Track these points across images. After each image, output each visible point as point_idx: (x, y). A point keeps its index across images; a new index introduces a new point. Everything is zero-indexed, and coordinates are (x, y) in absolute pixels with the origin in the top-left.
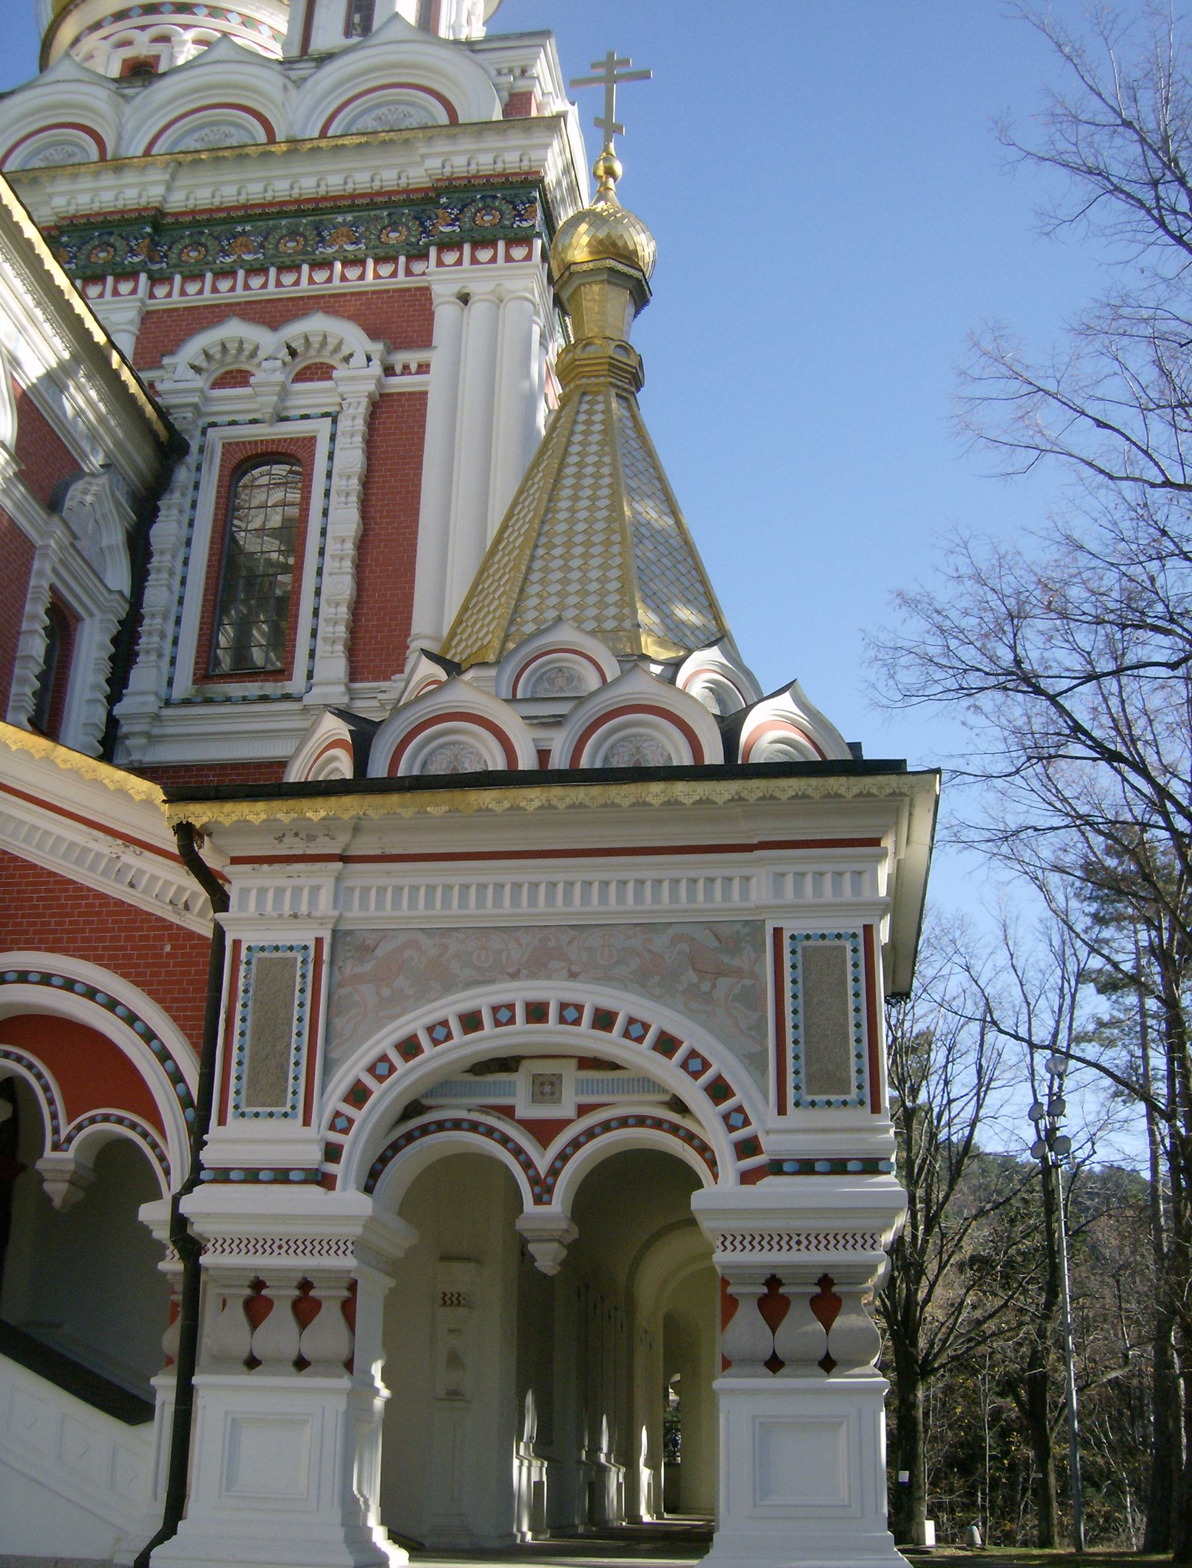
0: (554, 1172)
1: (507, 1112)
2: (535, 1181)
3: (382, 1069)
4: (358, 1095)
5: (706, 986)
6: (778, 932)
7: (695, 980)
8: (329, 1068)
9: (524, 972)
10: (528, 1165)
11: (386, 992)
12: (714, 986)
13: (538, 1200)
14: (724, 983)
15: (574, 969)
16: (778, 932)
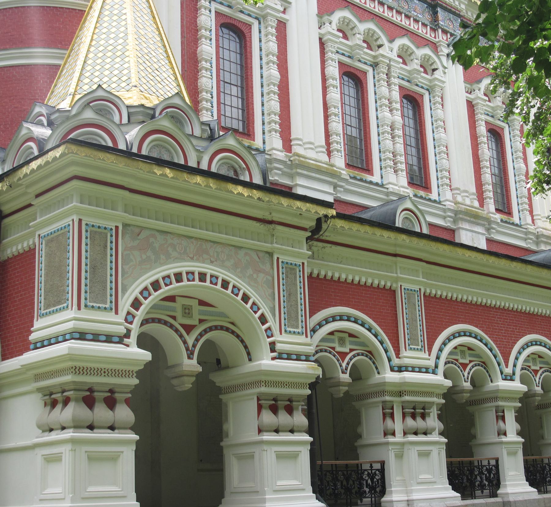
0: (194, 346)
1: (174, 318)
2: (187, 349)
3: (146, 294)
4: (136, 304)
5: (255, 276)
6: (278, 258)
7: (252, 273)
8: (124, 290)
9: (195, 258)
10: (185, 342)
11: (144, 257)
12: (257, 277)
13: (189, 358)
14: (261, 275)
15: (212, 259)
16: (278, 258)
